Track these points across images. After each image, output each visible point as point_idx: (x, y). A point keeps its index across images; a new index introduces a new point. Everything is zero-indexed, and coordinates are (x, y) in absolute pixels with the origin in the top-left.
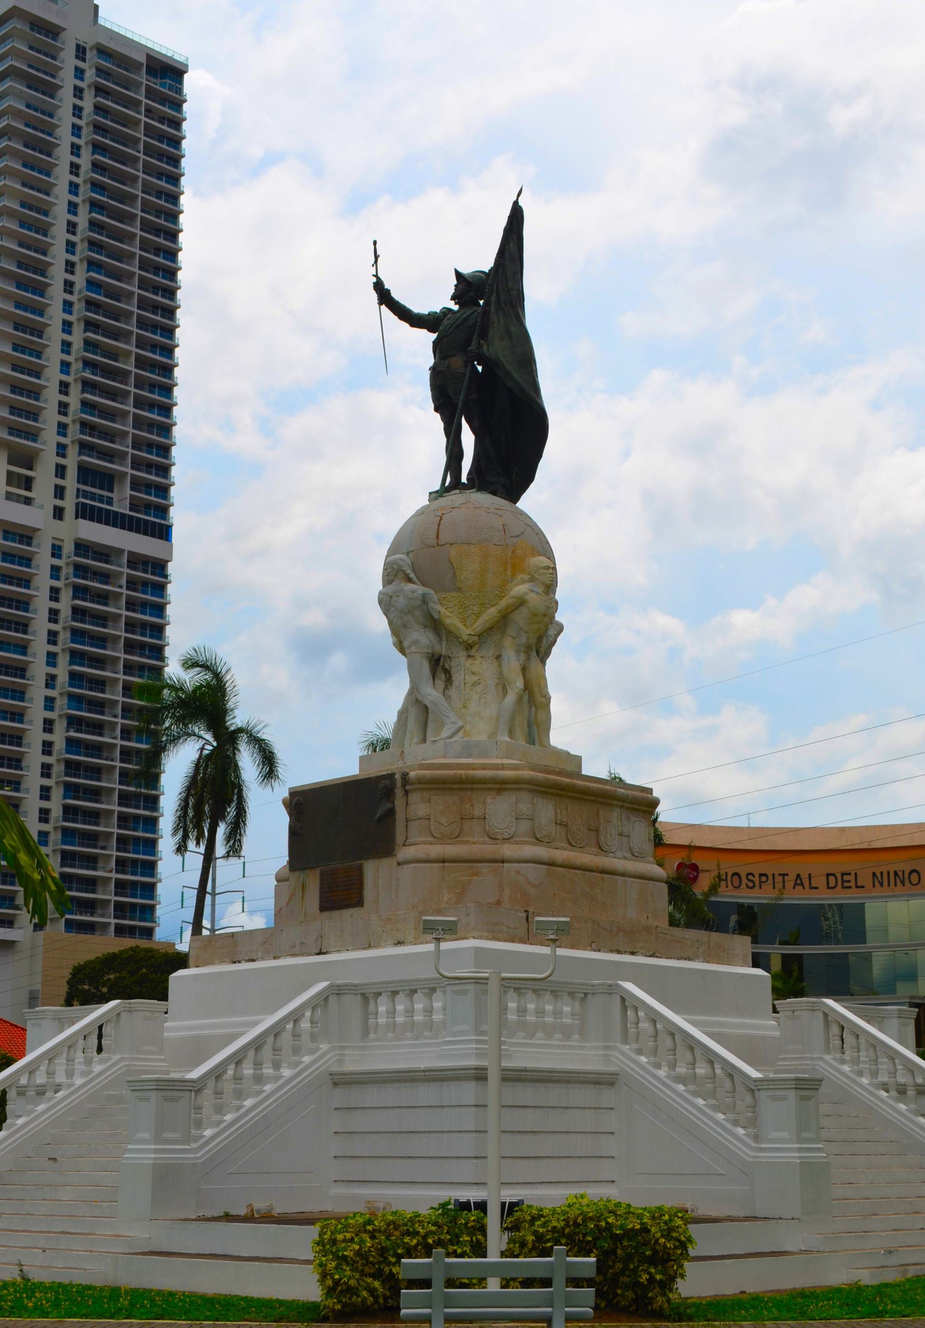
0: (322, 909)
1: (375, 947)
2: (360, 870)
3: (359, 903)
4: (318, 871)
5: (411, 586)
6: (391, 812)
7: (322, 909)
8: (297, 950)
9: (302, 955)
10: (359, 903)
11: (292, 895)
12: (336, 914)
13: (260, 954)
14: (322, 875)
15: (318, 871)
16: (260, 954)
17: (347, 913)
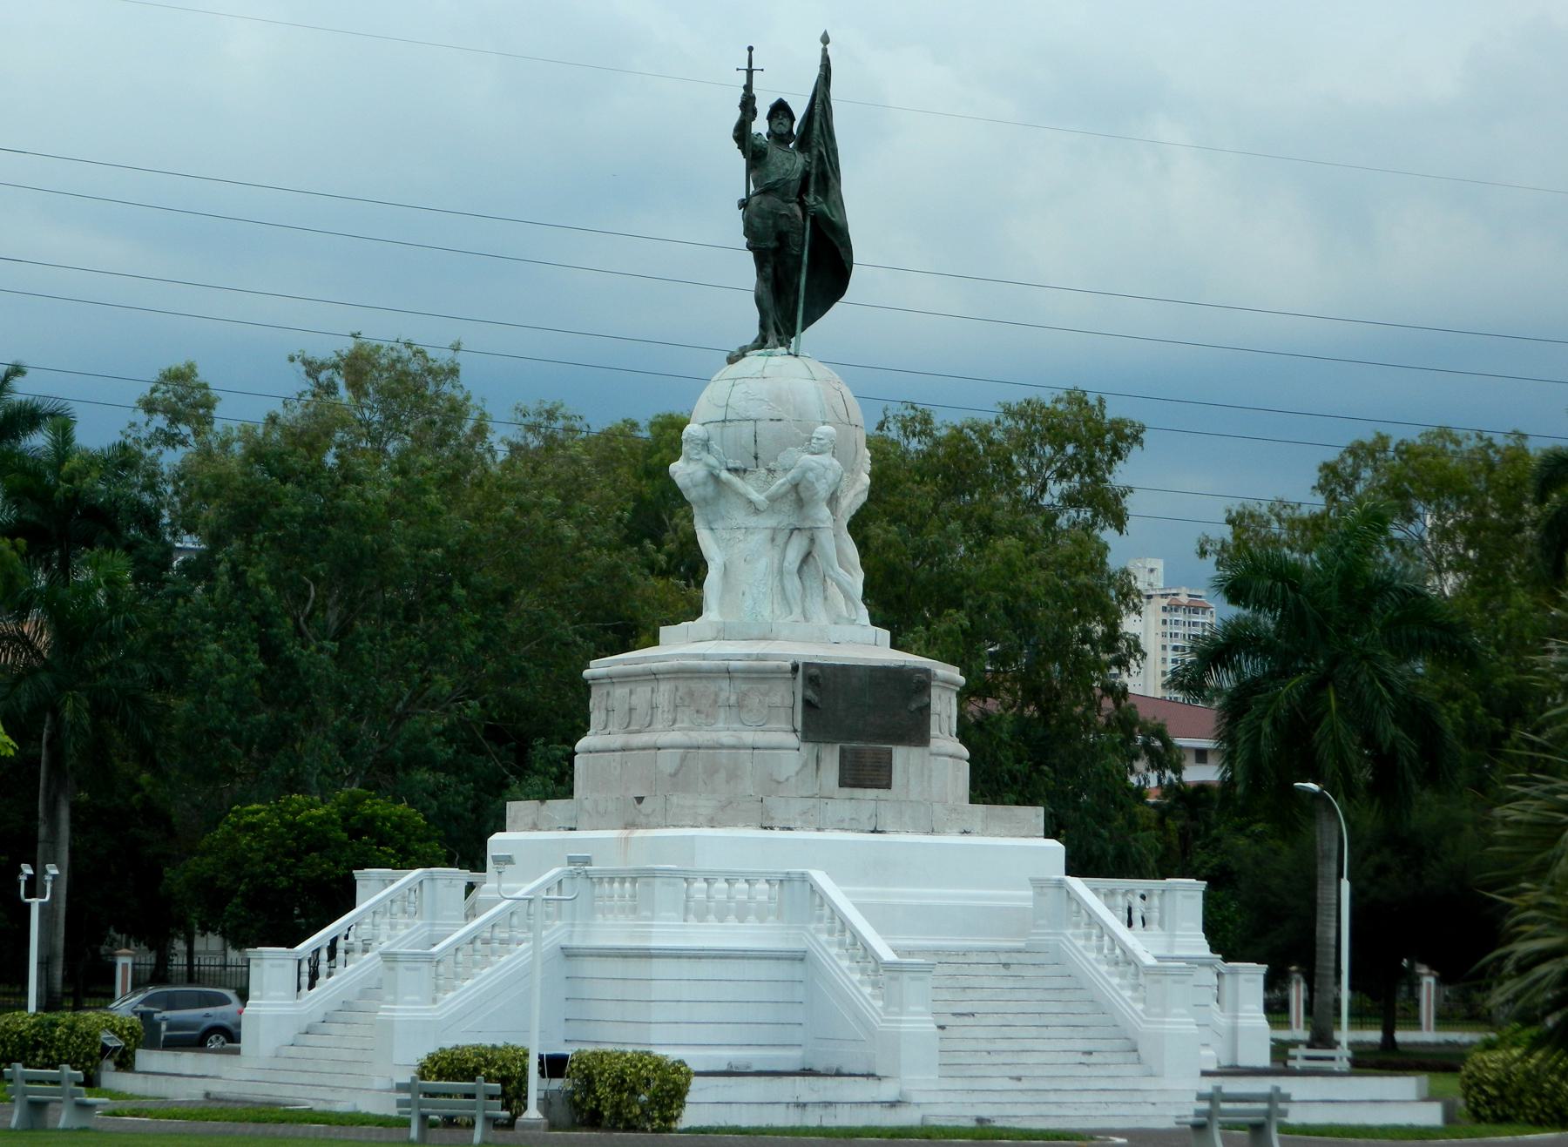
0: (842, 784)
1: (939, 833)
2: (890, 753)
3: (888, 786)
4: (837, 747)
5: (835, 462)
6: (928, 706)
7: (842, 784)
8: (846, 825)
9: (853, 830)
10: (888, 786)
11: (805, 765)
12: (858, 792)
13: (799, 824)
14: (842, 751)
15: (837, 747)
16: (799, 824)
17: (871, 793)
